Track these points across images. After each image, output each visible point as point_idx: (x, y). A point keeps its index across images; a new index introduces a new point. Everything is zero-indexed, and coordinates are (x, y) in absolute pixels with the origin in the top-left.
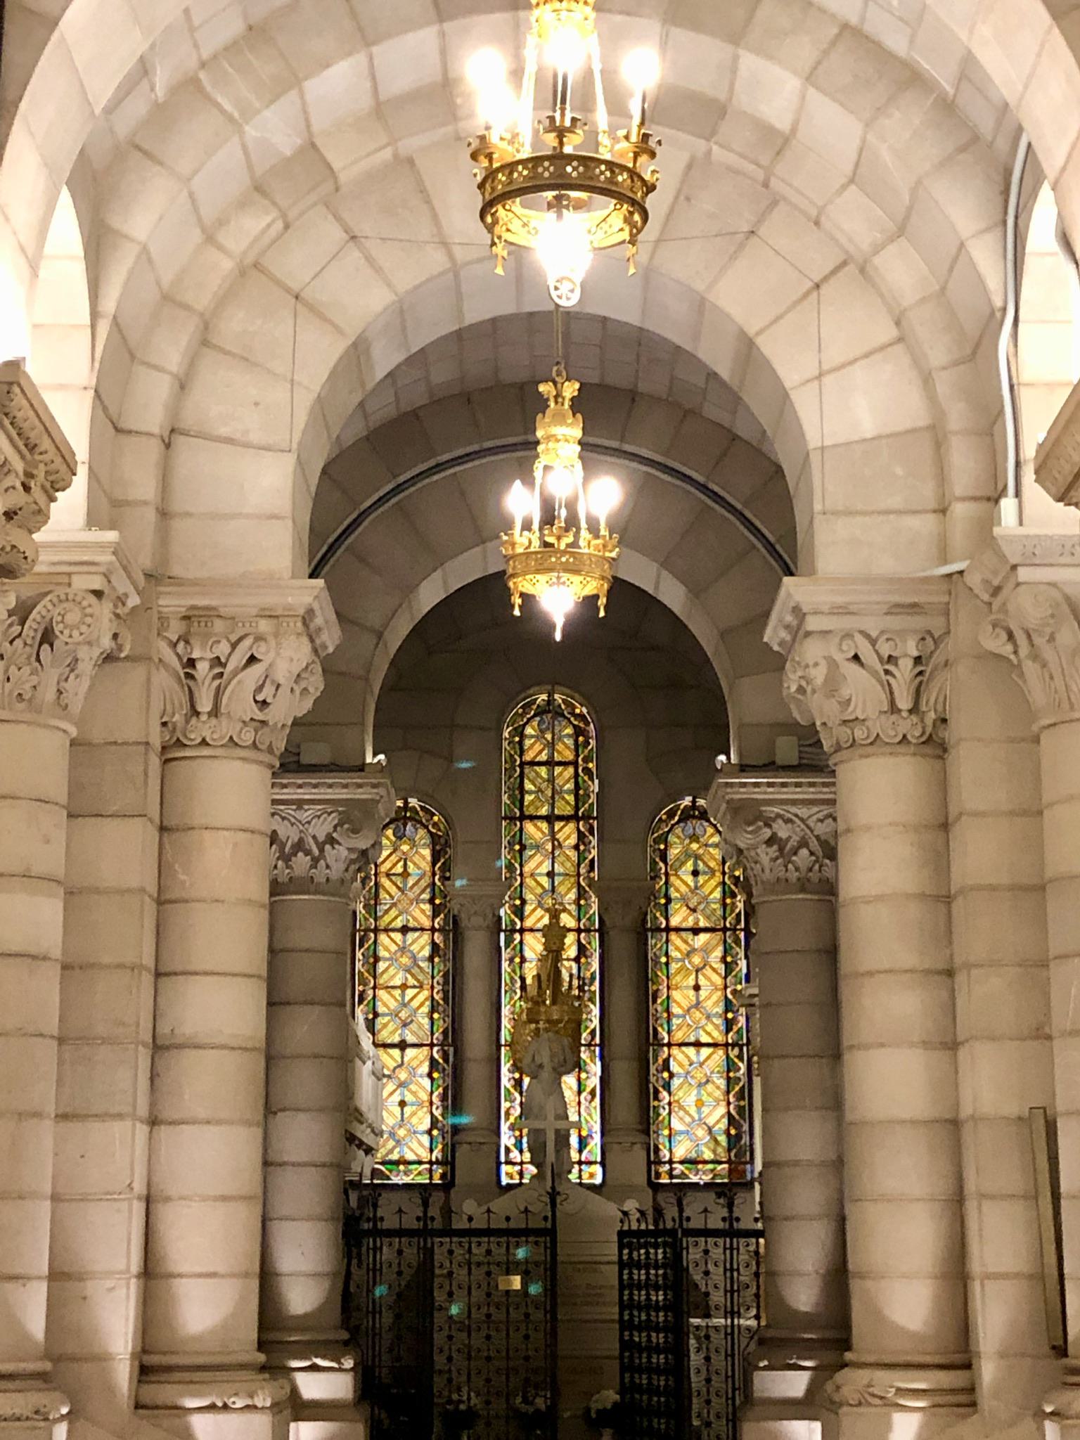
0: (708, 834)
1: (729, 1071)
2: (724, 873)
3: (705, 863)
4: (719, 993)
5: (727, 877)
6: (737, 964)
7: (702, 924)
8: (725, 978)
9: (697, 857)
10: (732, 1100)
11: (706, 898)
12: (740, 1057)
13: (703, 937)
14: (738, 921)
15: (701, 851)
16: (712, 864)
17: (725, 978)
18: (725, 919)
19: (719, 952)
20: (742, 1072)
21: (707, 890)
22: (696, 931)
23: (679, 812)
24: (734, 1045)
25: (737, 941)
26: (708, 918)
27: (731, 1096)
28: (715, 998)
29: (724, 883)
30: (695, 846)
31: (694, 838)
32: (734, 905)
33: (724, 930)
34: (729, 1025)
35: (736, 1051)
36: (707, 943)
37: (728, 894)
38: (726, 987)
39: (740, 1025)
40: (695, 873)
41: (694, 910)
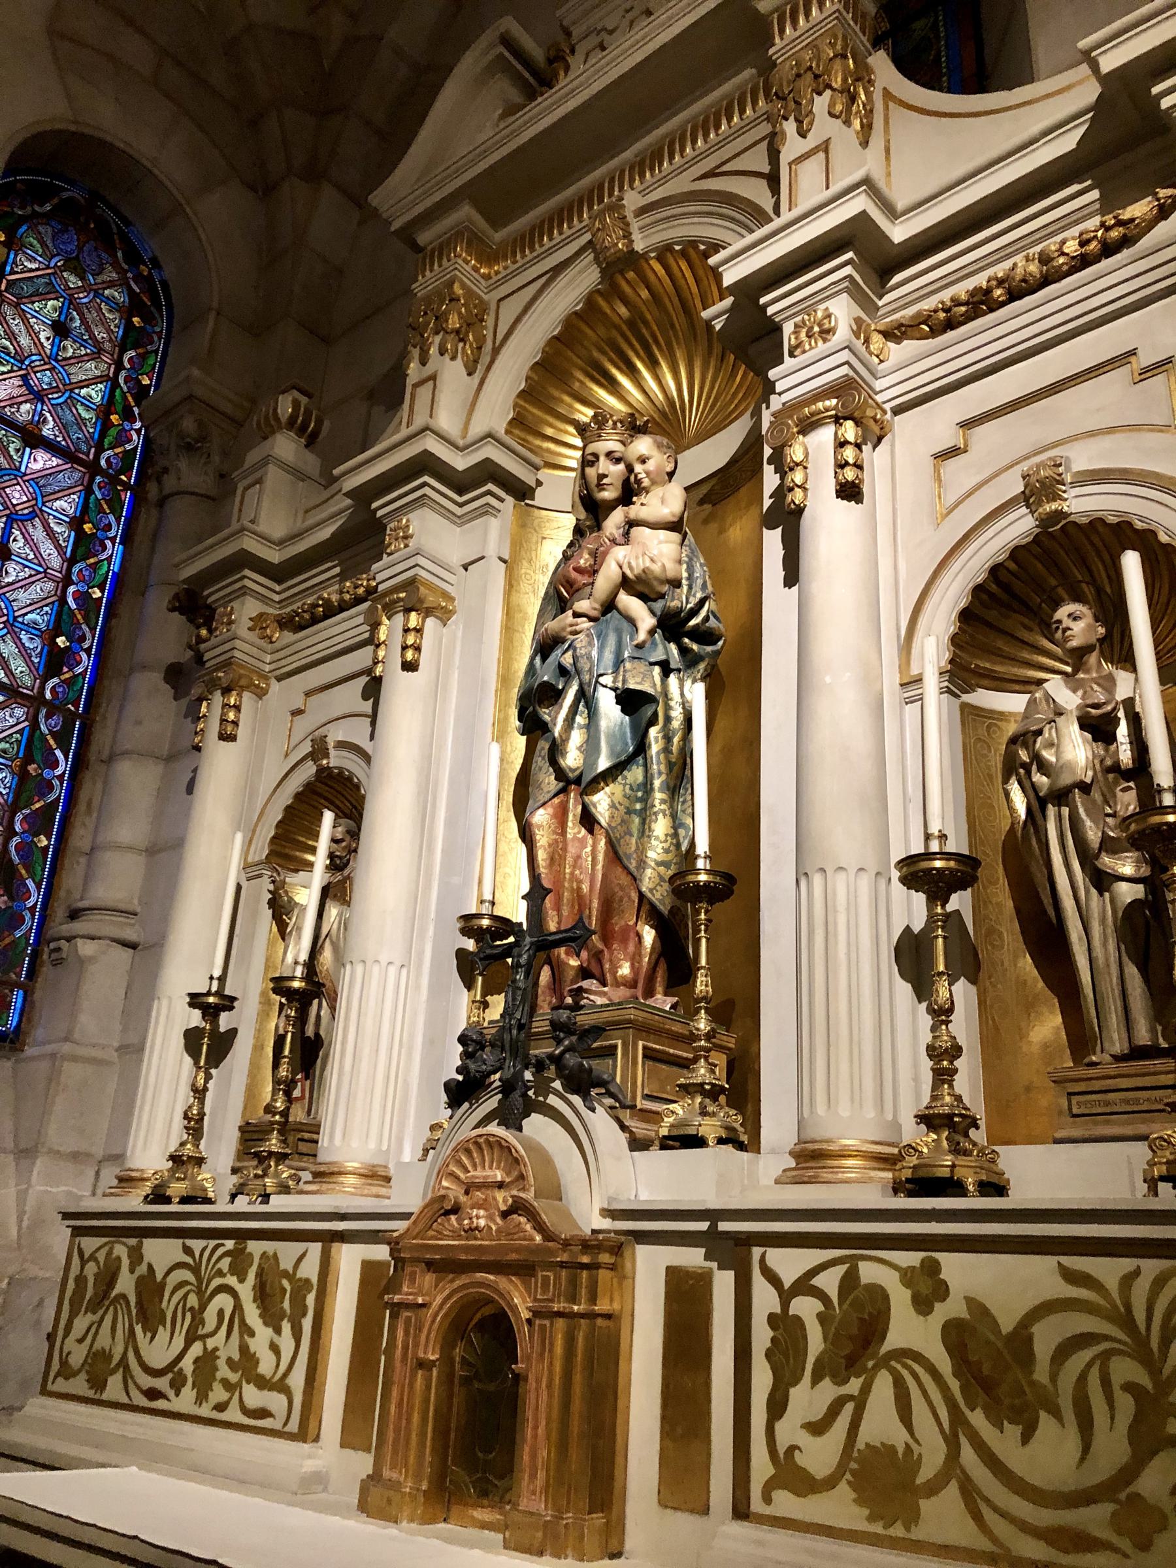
0: (105, 277)
1: (28, 759)
2: (119, 366)
3: (84, 321)
4: (50, 586)
5: (123, 374)
6: (104, 548)
7: (48, 430)
8: (72, 562)
9: (72, 302)
10: (18, 828)
11: (71, 387)
12: (62, 737)
13: (41, 461)
14: (127, 470)
15: (84, 298)
16: (100, 334)
17: (72, 562)
18: (100, 449)
19: (67, 505)
20: (59, 771)
21: (78, 374)
22: (32, 439)
23: (55, 201)
24: (53, 708)
25: (115, 504)
26: (64, 427)
27: (19, 817)
28: (38, 590)
29: (115, 385)
30: (73, 281)
31: (74, 265)
32: (123, 437)
33: (93, 468)
34: (55, 661)
35: (57, 721)
36: (48, 475)
37: (119, 408)
38: (67, 581)
39: (79, 670)
40: (60, 329)
41: (38, 396)
